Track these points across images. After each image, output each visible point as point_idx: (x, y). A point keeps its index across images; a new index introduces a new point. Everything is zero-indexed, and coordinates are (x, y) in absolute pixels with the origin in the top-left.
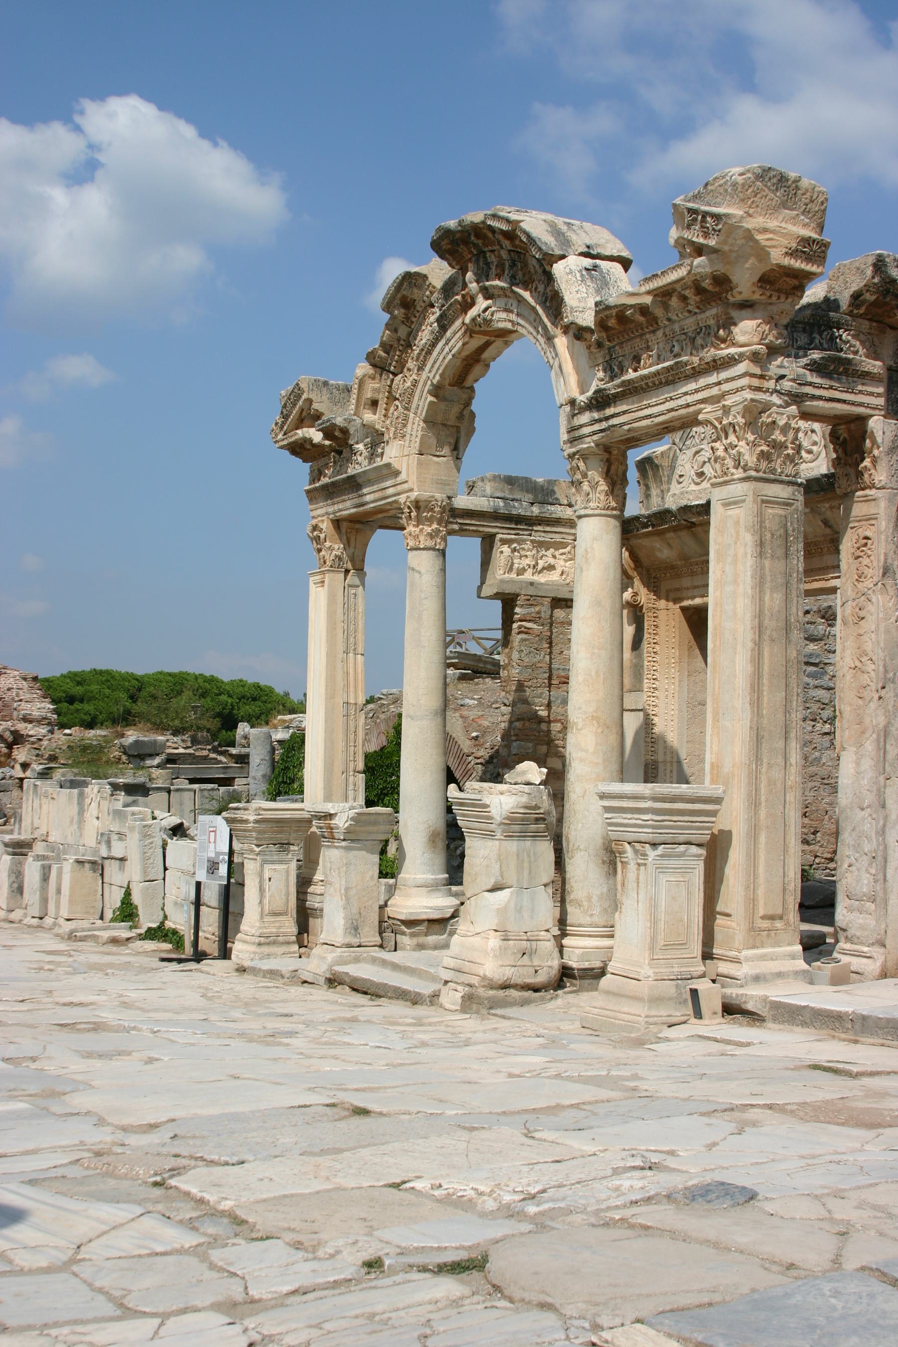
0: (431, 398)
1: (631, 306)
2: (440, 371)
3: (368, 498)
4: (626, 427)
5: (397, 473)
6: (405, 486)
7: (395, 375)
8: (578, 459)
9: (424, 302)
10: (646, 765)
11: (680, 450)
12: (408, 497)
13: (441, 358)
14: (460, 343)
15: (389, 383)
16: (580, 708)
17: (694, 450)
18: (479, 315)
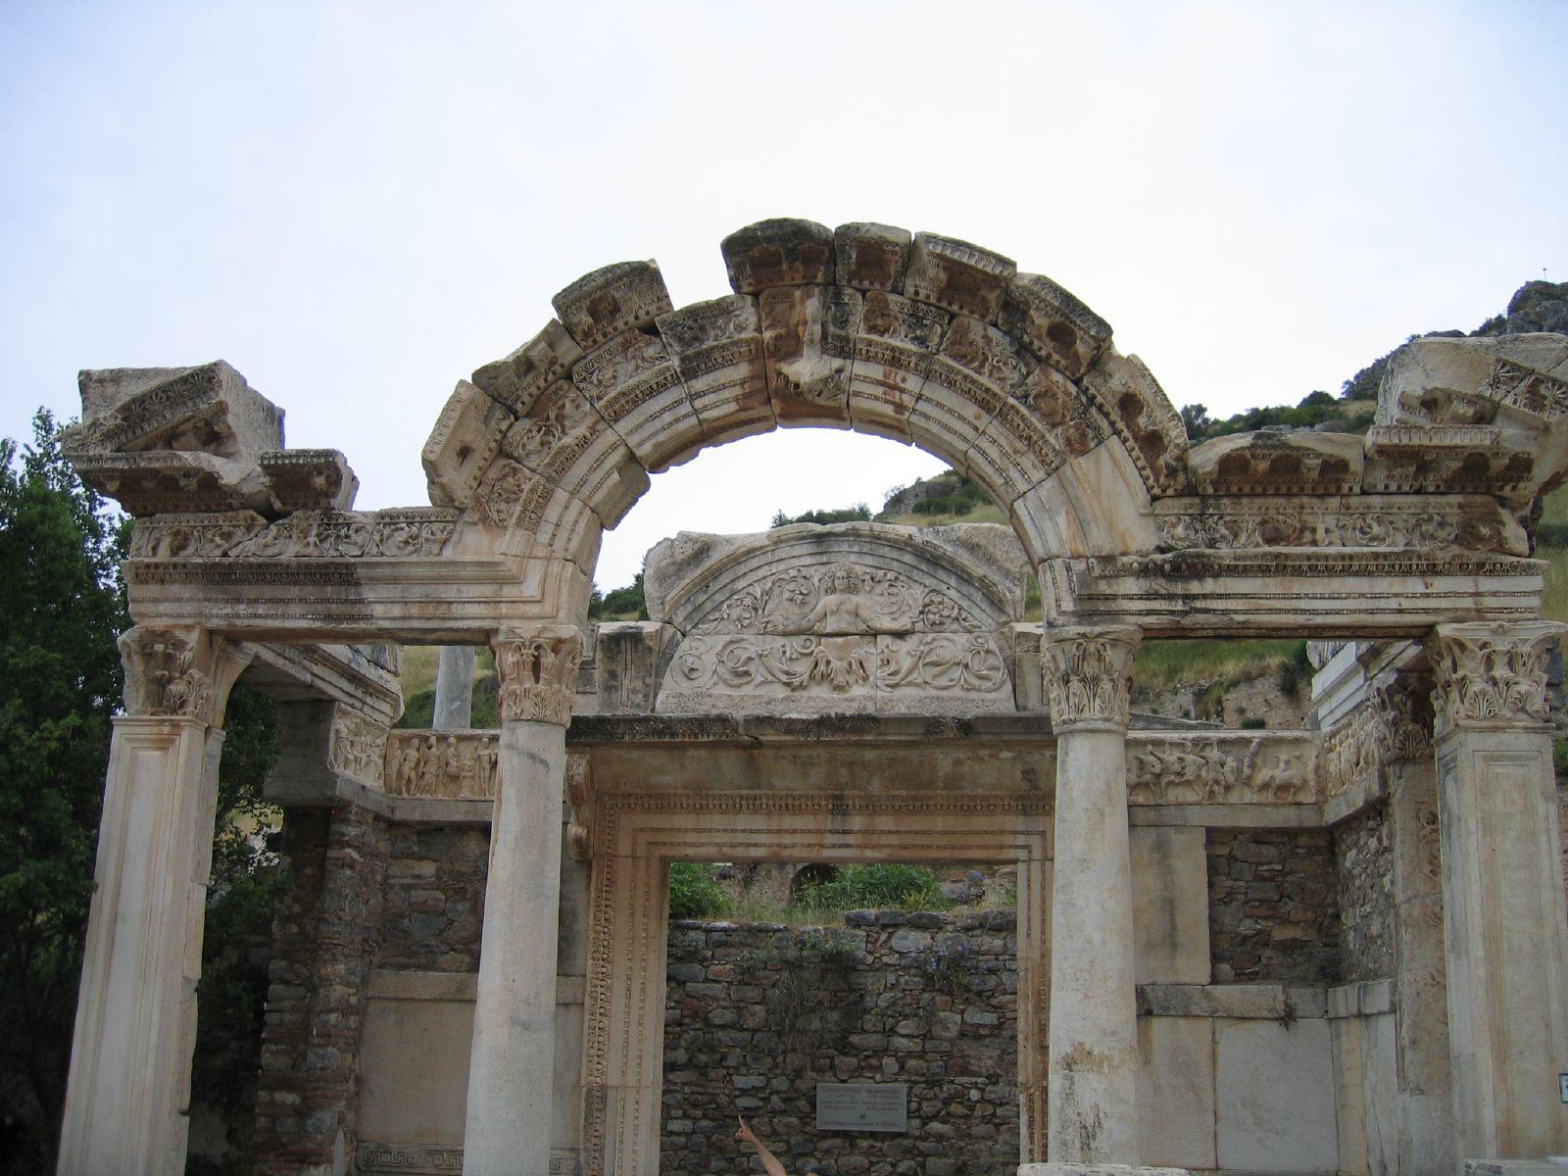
0: (616, 477)
1: (1319, 455)
2: (661, 437)
3: (378, 610)
4: (1240, 618)
5: (514, 580)
6: (534, 610)
7: (517, 419)
8: (1103, 644)
9: (637, 318)
10: (589, 1091)
11: (684, 635)
12: (544, 629)
13: (667, 417)
14: (733, 407)
15: (504, 426)
16: (1114, 1033)
17: (728, 638)
18: (832, 377)
